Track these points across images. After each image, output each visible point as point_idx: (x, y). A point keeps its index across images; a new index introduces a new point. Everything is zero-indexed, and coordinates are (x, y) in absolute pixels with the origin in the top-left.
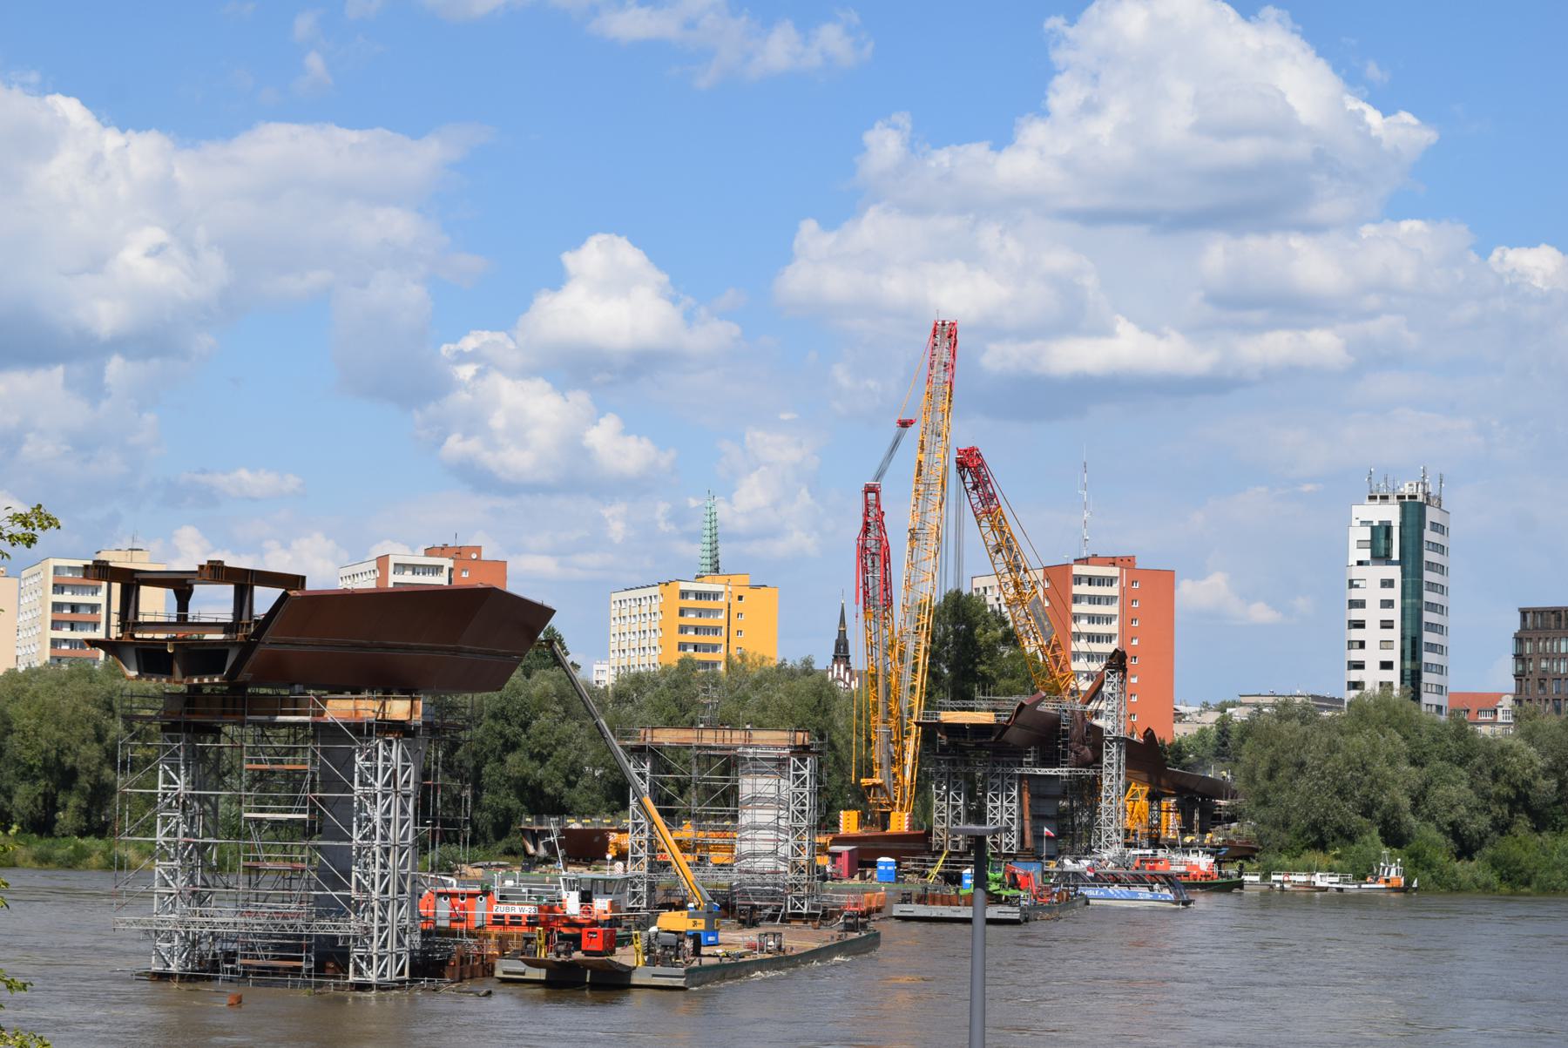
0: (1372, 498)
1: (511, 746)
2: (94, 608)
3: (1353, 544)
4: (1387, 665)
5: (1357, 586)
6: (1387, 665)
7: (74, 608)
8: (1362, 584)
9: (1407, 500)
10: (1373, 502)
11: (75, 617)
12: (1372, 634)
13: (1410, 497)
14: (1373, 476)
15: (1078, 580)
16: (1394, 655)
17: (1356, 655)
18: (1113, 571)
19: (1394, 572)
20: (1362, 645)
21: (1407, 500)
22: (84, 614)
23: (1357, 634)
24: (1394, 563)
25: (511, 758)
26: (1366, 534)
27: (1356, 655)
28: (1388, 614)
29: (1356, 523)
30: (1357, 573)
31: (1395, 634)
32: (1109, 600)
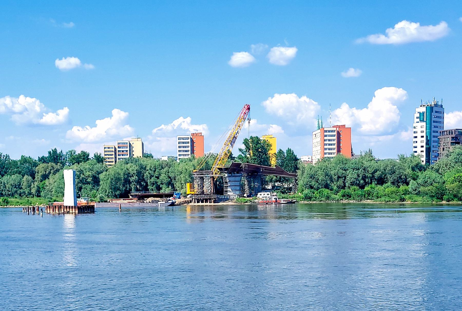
0: (421, 106)
1: (152, 176)
2: (127, 151)
3: (415, 118)
4: (422, 147)
5: (415, 128)
6: (422, 147)
7: (123, 151)
8: (416, 127)
9: (429, 106)
10: (421, 107)
11: (123, 153)
12: (419, 139)
13: (430, 105)
14: (422, 101)
15: (326, 131)
16: (424, 144)
17: (415, 145)
18: (335, 129)
19: (424, 124)
20: (416, 142)
21: (429, 106)
22: (125, 153)
23: (415, 140)
24: (425, 122)
25: (153, 178)
26: (418, 115)
27: (415, 145)
28: (423, 134)
29: (417, 113)
30: (415, 125)
31: (424, 139)
32: (334, 136)
